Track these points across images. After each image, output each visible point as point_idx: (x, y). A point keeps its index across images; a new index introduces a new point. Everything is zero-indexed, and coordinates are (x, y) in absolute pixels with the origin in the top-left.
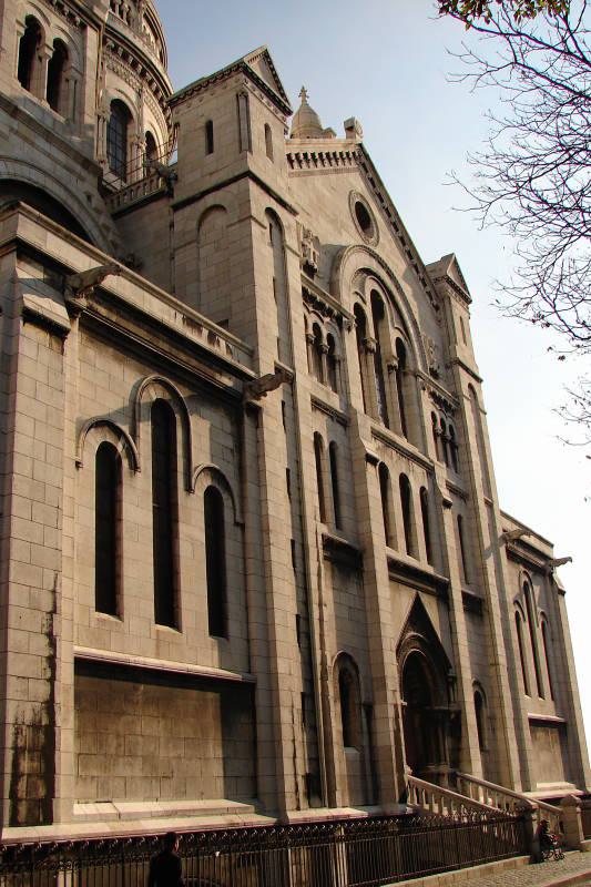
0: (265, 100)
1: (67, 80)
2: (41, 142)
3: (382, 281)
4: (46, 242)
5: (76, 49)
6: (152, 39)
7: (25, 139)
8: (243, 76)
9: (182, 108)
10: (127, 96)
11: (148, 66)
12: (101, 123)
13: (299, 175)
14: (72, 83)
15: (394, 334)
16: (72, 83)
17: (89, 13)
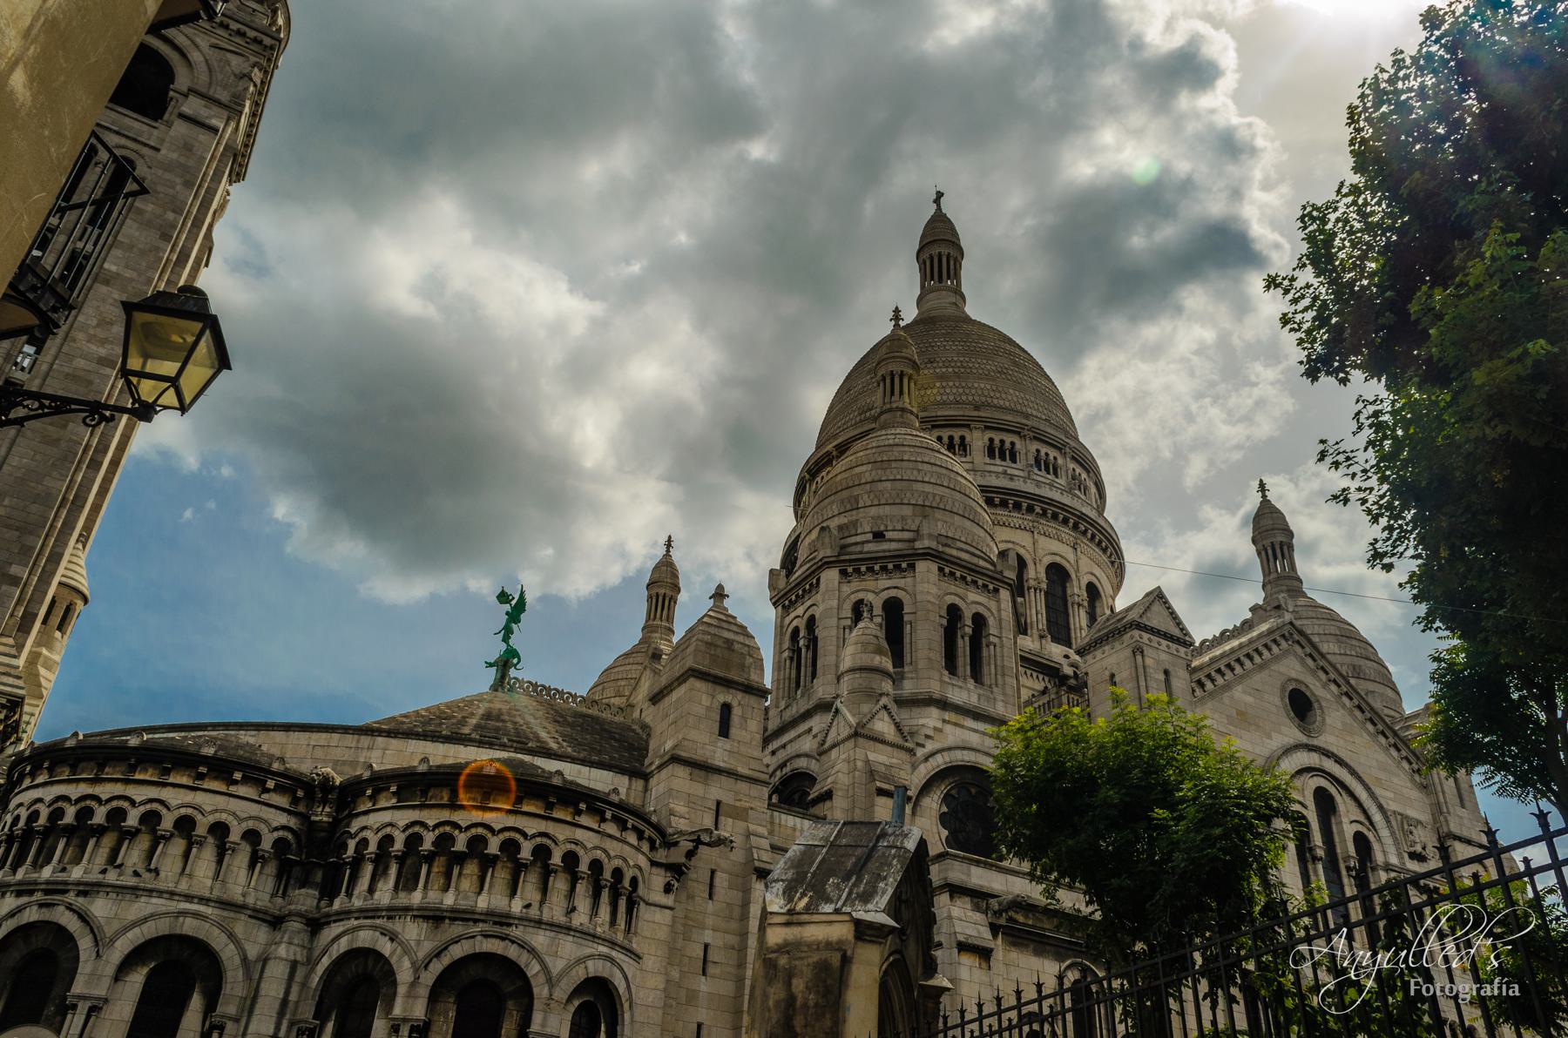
0: (1164, 643)
1: (988, 646)
2: (969, 723)
3: (1329, 774)
4: (969, 875)
5: (992, 614)
6: (1084, 476)
7: (956, 724)
8: (1136, 633)
9: (1089, 657)
10: (1061, 556)
11: (1079, 517)
12: (1038, 595)
13: (1212, 695)
14: (992, 647)
15: (1350, 830)
16: (992, 647)
17: (999, 577)
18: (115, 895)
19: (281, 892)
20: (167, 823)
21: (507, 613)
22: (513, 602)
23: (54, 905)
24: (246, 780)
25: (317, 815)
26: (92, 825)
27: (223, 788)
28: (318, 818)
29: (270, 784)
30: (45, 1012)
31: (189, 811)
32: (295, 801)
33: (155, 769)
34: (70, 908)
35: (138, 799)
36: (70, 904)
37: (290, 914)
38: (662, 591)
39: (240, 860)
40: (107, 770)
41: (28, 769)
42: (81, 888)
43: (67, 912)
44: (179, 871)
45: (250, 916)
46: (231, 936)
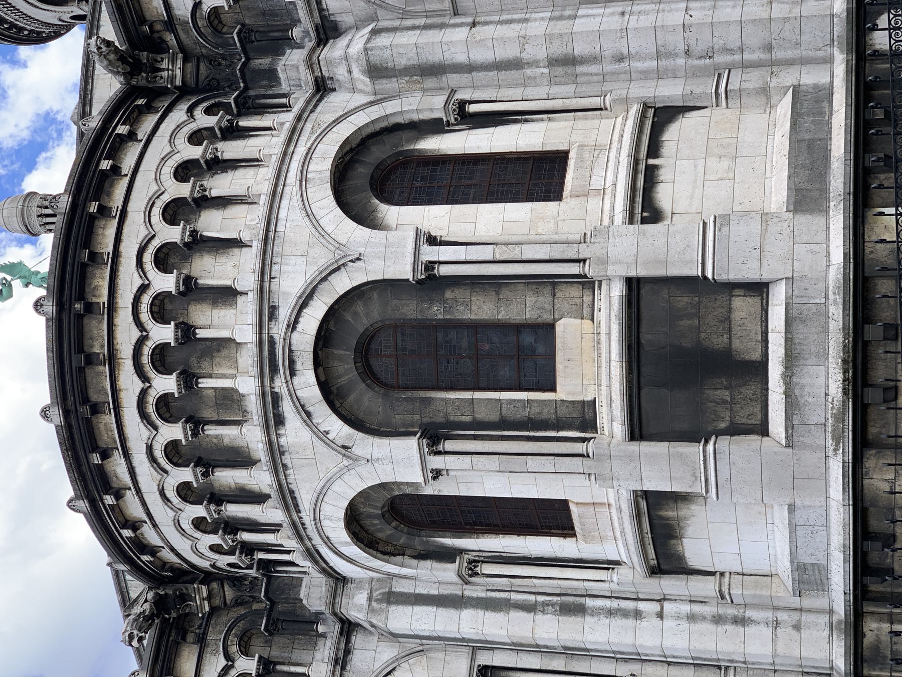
18: (275, 267)
19: (283, 101)
20: (173, 234)
21: (27, 285)
22: (9, 278)
23: (291, 351)
24: (115, 153)
25: (173, 77)
26: (176, 339)
27: (126, 180)
28: (178, 73)
29: (122, 129)
30: (440, 317)
31: (157, 211)
32: (149, 108)
33: (94, 276)
34: (293, 326)
35: (138, 282)
36: (288, 326)
37: (311, 67)
38: (35, 211)
39: (230, 149)
40: (96, 350)
41: (109, 500)
42: (266, 318)
43: (299, 327)
44: (246, 207)
45: (312, 111)
46: (337, 121)
